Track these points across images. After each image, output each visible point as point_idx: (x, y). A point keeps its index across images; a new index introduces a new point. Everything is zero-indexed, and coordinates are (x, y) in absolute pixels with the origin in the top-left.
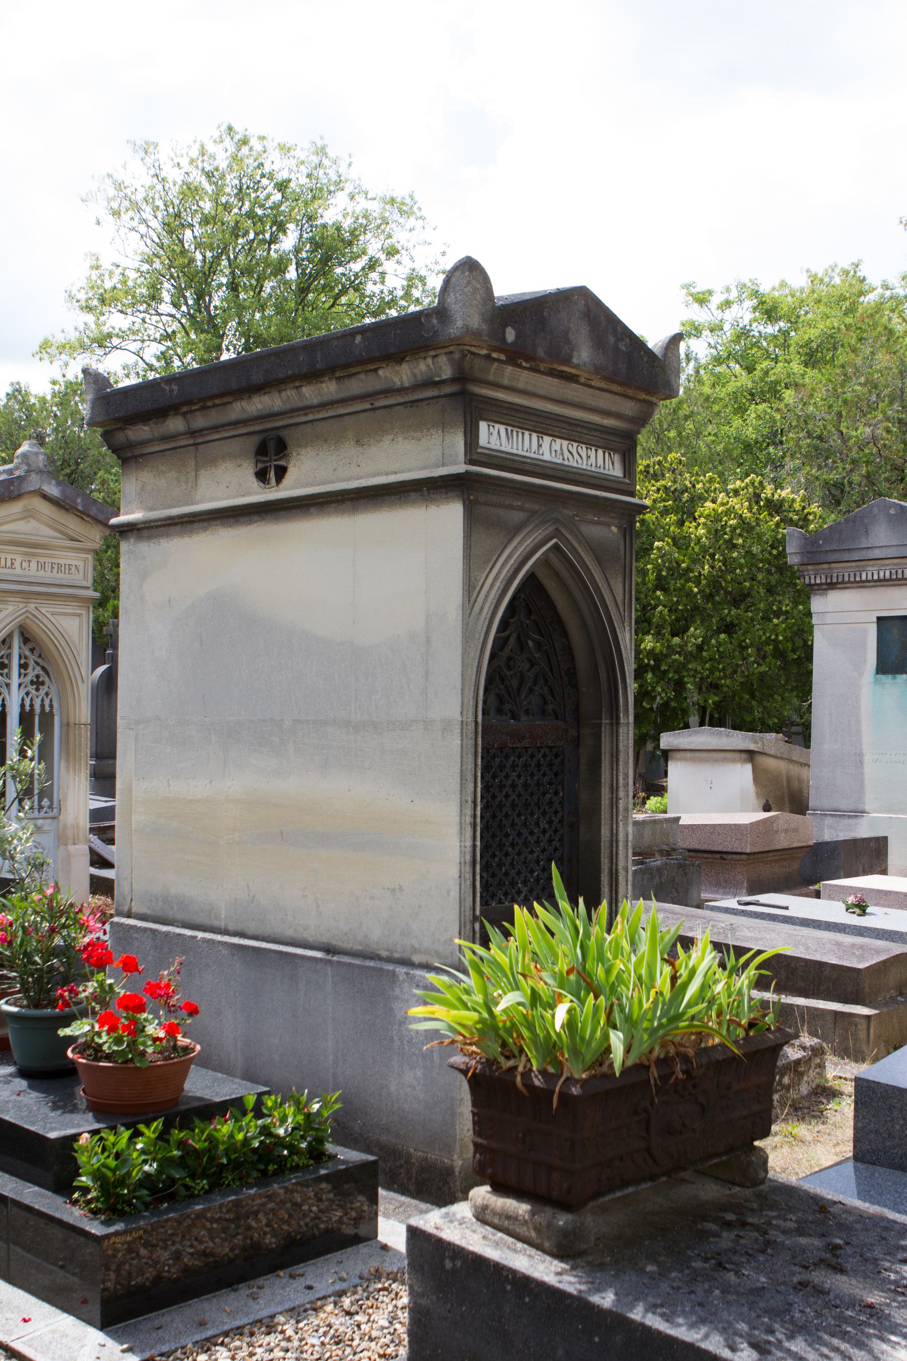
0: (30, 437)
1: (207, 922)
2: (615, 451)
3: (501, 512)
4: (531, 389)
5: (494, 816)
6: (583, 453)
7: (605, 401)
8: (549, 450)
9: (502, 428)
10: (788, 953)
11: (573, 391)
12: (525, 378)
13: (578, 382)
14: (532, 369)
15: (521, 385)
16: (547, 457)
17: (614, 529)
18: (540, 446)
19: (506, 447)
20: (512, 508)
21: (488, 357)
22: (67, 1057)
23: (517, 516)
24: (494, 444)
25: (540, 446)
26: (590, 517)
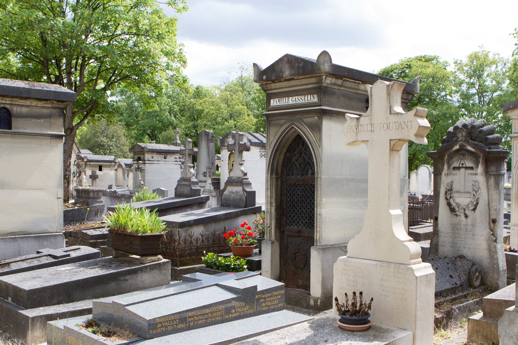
0: (149, 129)
1: (45, 232)
2: (314, 94)
3: (278, 121)
4: (280, 87)
5: (311, 212)
6: (303, 98)
7: (304, 81)
8: (291, 101)
9: (277, 99)
10: (273, 313)
11: (292, 83)
12: (278, 85)
13: (294, 80)
14: (279, 82)
15: (278, 87)
16: (291, 103)
17: (316, 118)
18: (288, 100)
19: (278, 104)
20: (281, 119)
21: (267, 84)
22: (160, 254)
23: (283, 121)
24: (275, 104)
25: (288, 100)
26: (306, 116)
